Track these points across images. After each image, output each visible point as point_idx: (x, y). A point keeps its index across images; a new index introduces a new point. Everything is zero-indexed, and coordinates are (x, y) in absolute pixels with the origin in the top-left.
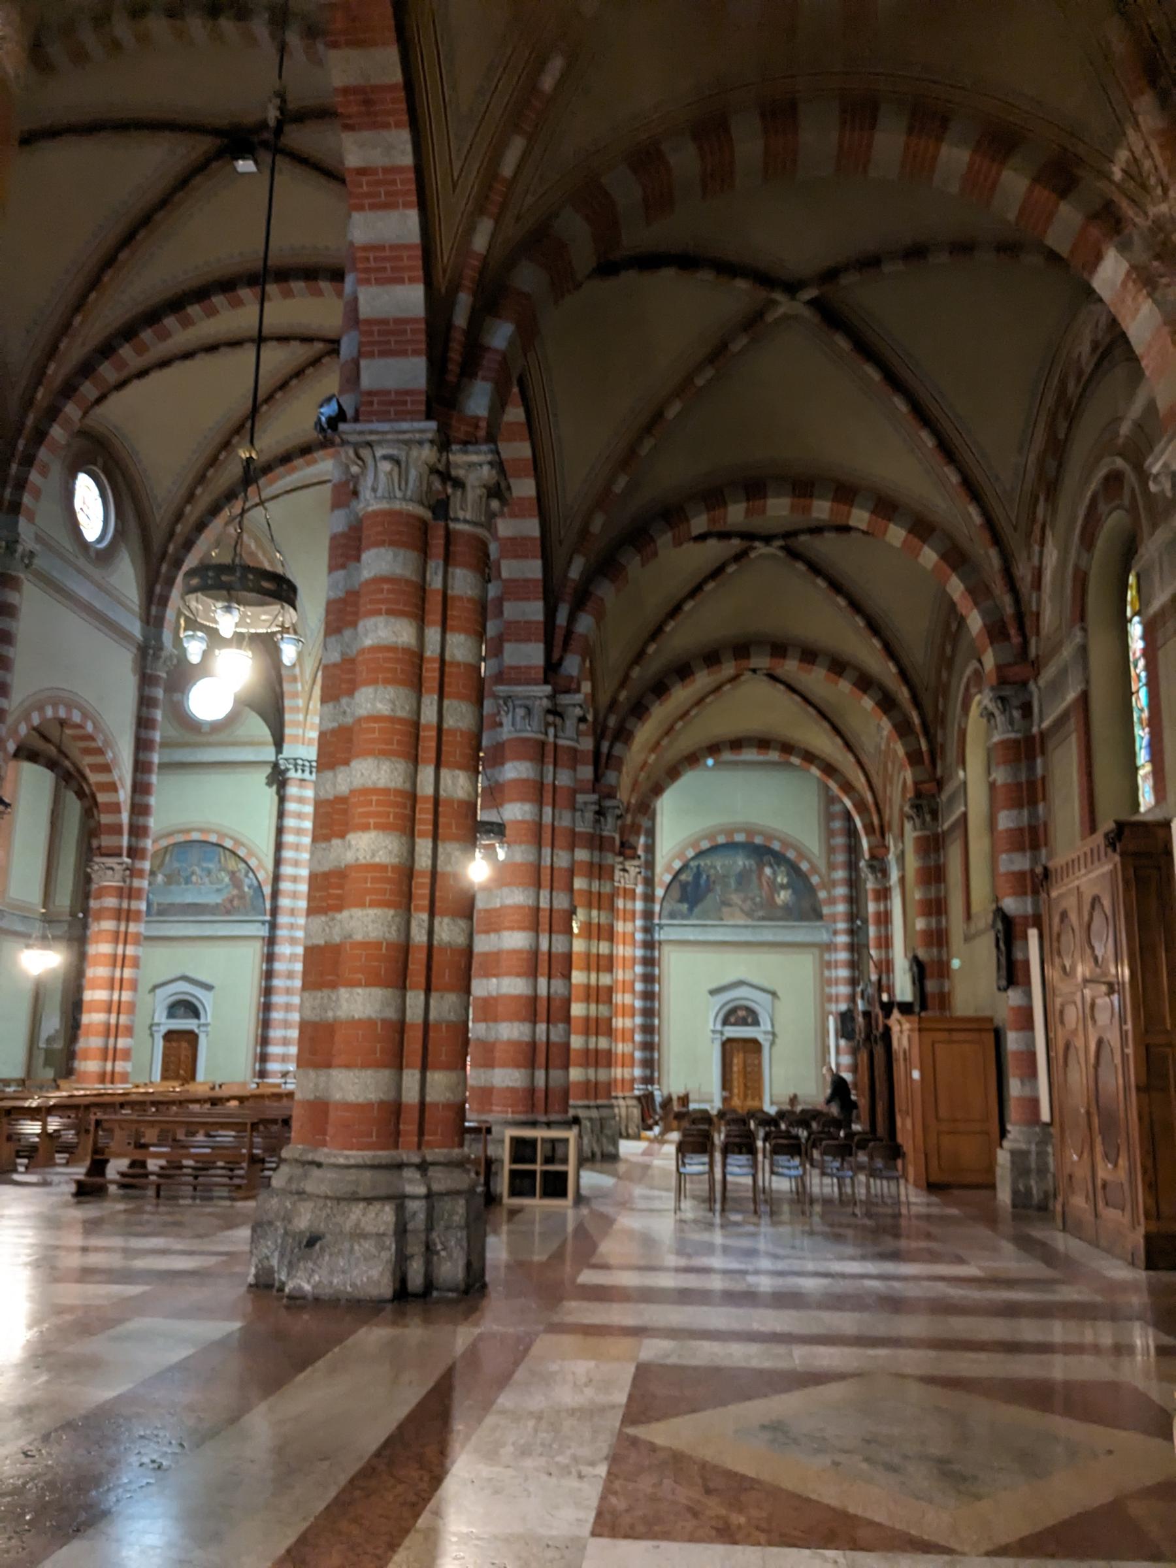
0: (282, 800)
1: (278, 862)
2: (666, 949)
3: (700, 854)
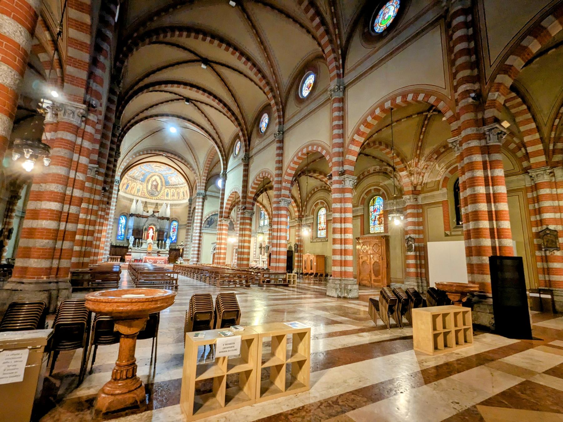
3: (212, 215)
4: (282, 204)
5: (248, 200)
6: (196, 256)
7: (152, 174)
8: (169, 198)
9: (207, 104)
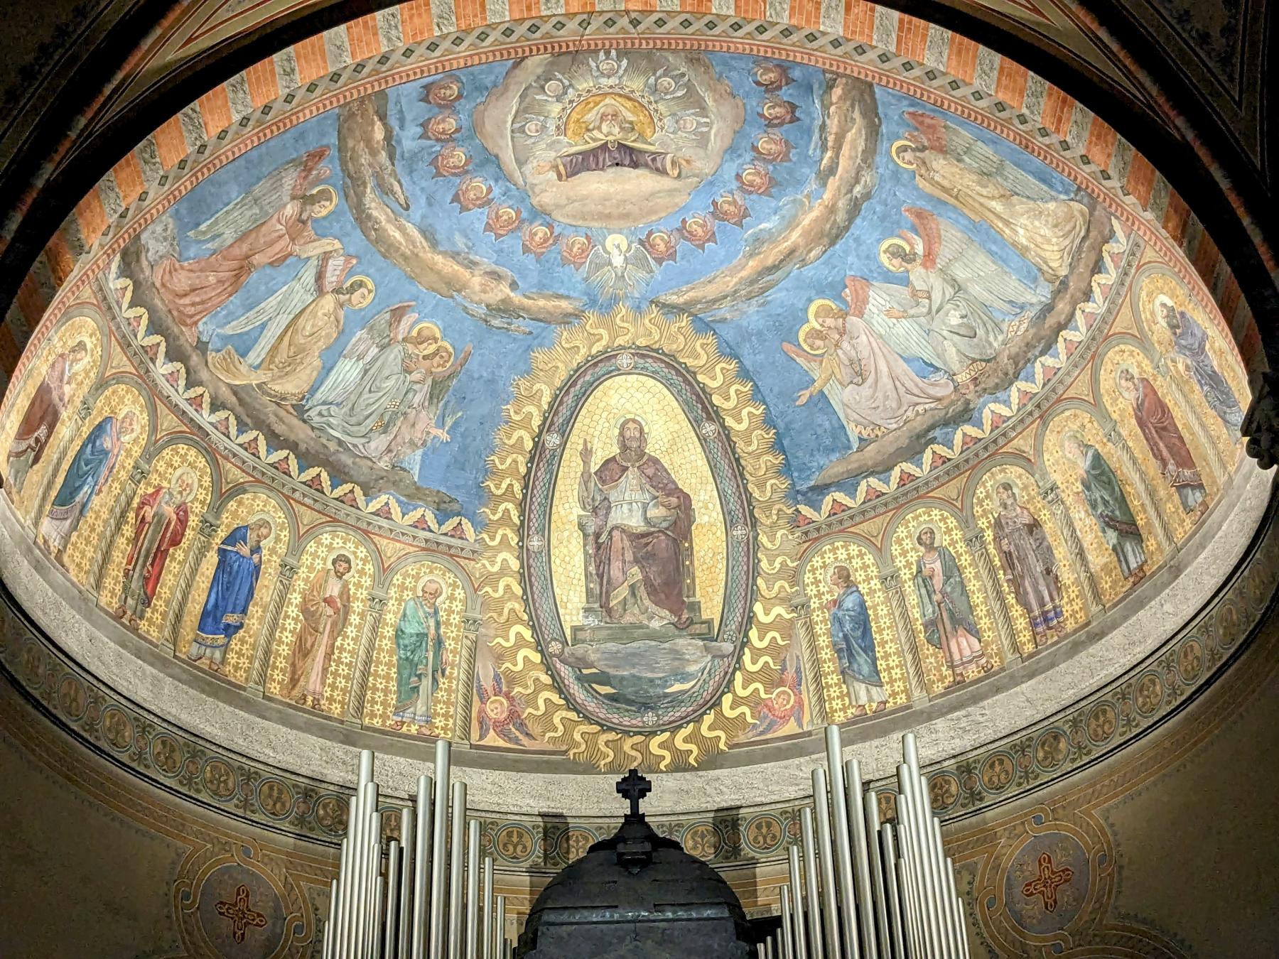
7: (563, 355)
8: (895, 682)
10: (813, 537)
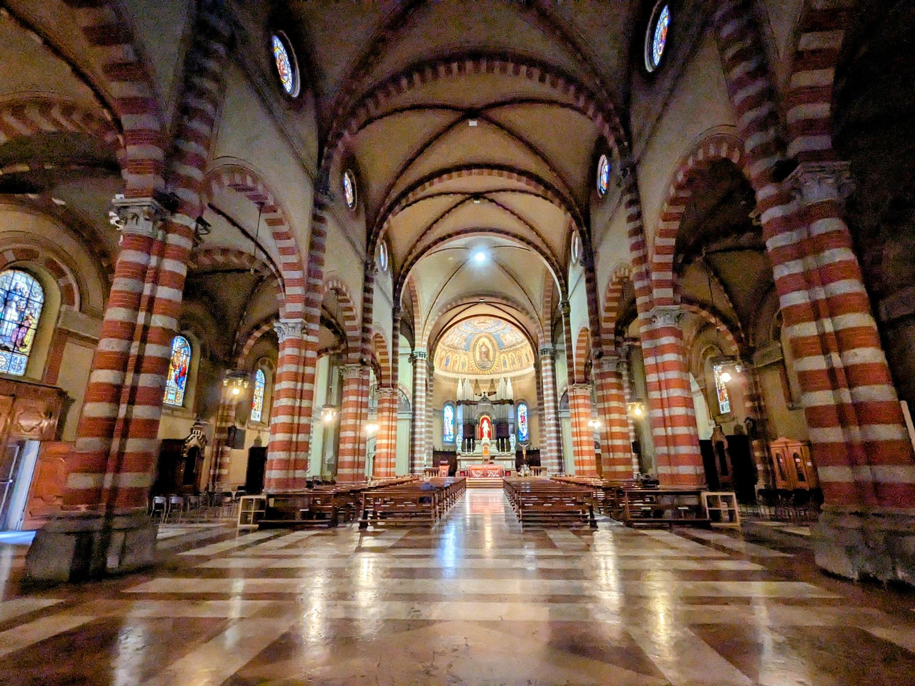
0: (415, 368)
1: (414, 391)
2: (563, 420)
4: (660, 323)
5: (604, 336)
6: (556, 461)
7: (477, 336)
8: (508, 368)
9: (505, 190)
10: (501, 353)
